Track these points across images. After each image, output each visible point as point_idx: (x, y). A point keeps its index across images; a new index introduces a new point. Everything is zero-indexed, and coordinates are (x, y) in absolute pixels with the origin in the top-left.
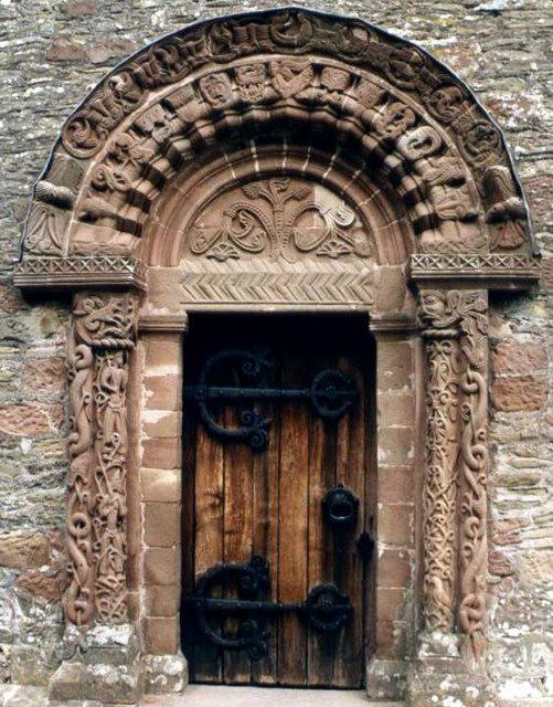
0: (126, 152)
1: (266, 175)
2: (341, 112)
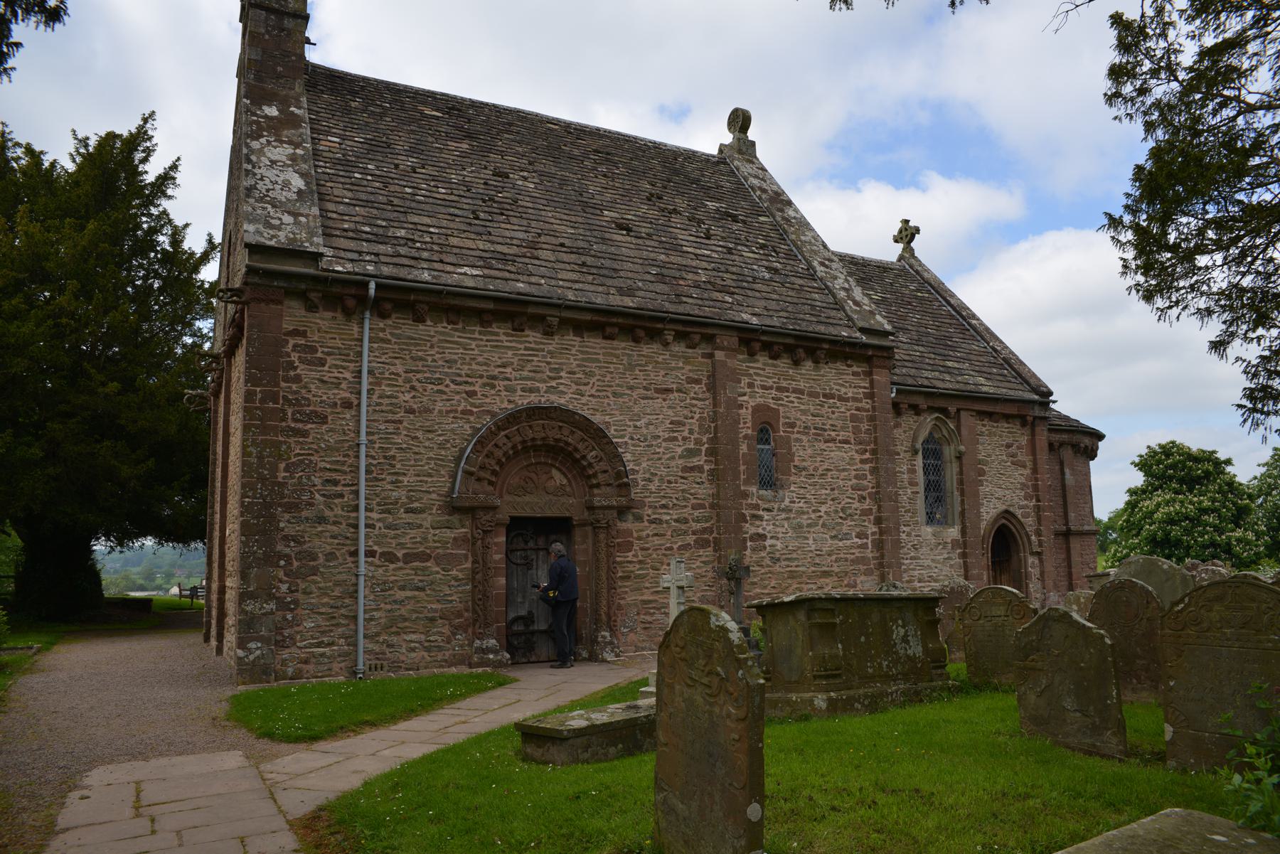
0: (492, 453)
1: (537, 463)
2: (567, 444)
